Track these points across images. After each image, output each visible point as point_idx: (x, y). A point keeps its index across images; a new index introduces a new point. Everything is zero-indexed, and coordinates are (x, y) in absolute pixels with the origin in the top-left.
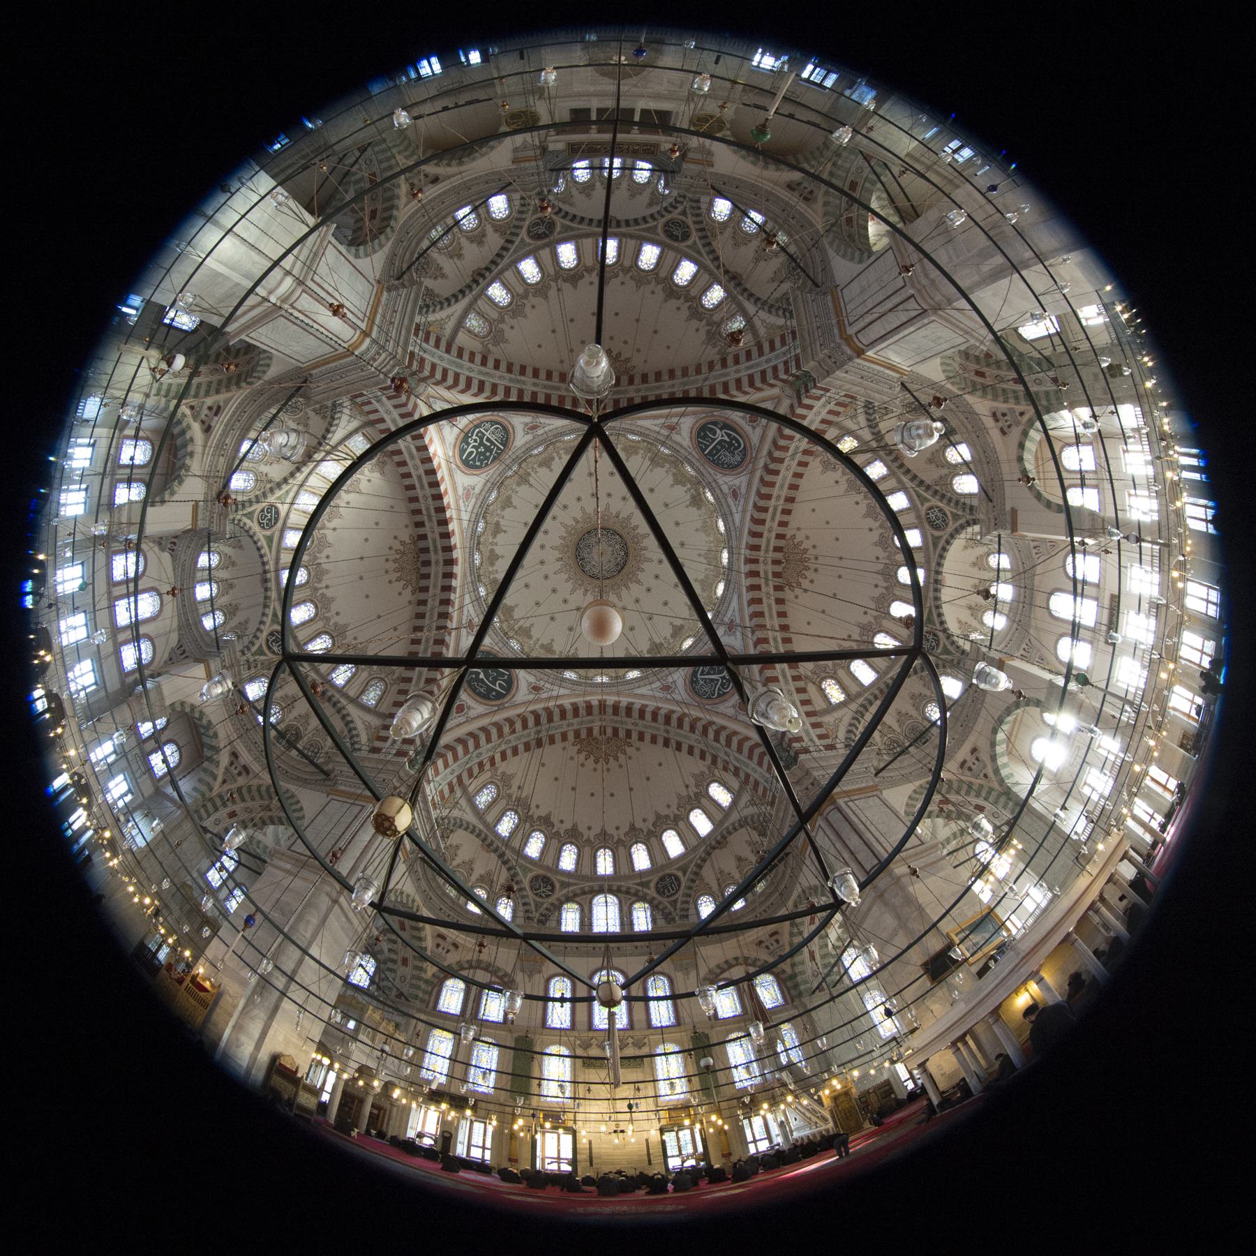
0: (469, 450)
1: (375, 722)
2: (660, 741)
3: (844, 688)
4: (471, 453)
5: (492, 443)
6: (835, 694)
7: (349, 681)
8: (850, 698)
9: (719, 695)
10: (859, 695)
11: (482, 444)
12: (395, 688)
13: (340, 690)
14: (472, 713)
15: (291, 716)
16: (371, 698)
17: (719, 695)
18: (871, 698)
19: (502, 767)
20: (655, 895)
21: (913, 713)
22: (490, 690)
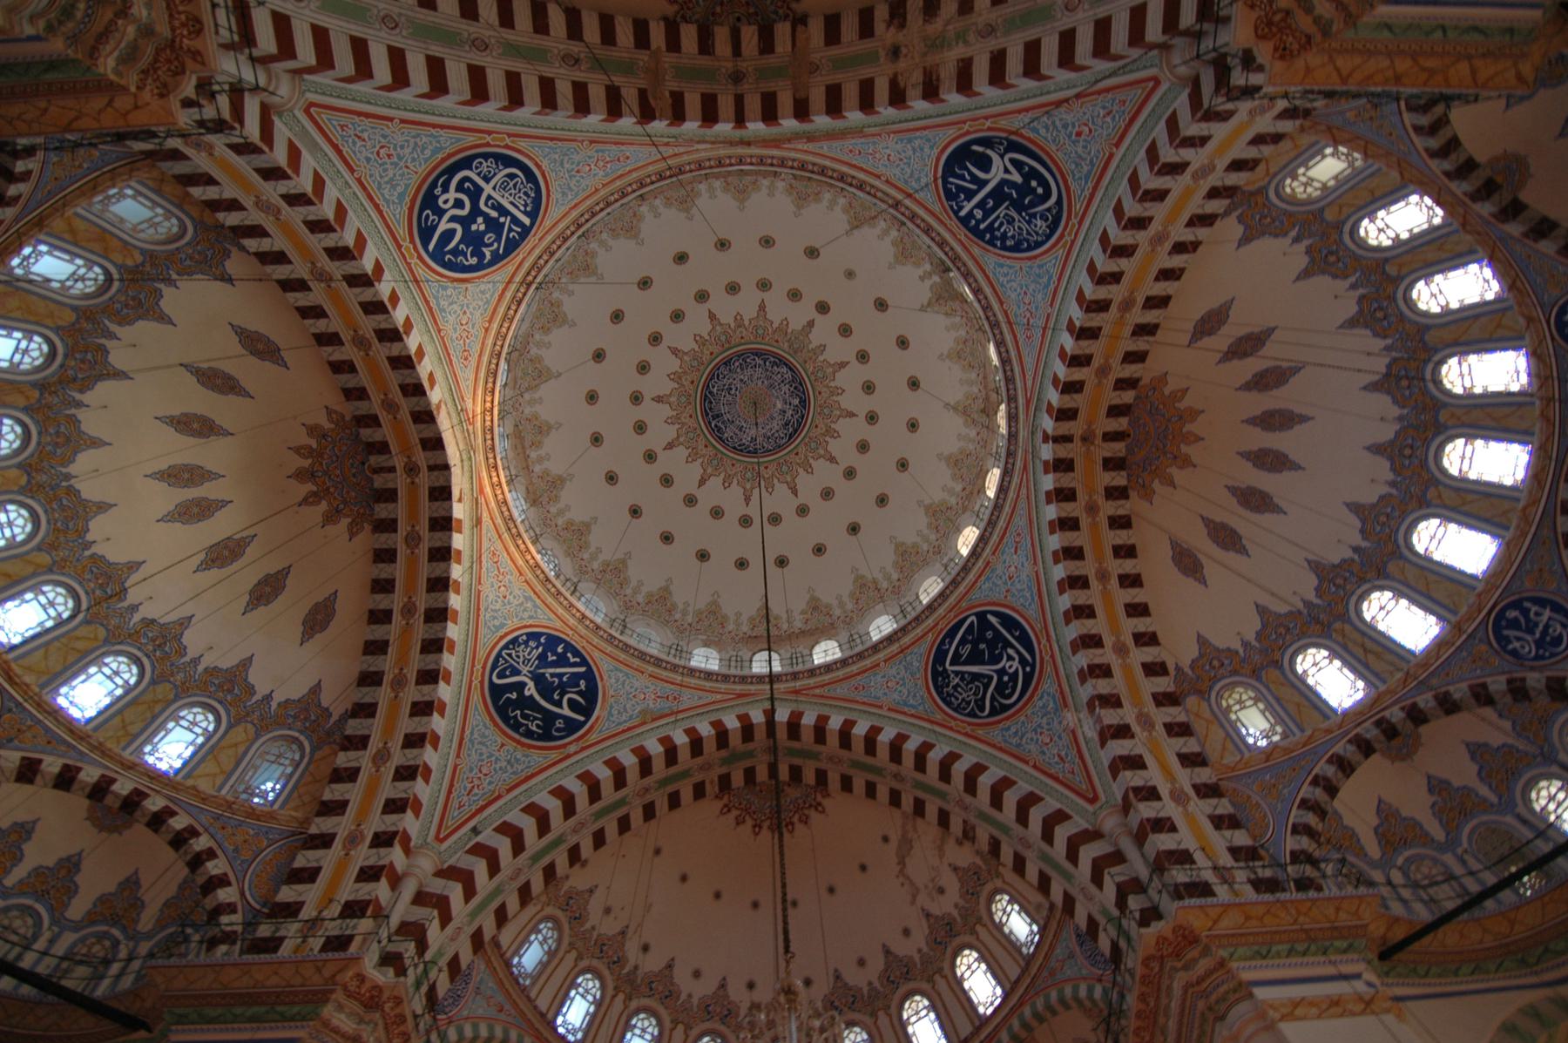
0: (444, 226)
2: (883, 792)
4: (449, 235)
5: (503, 211)
6: (1255, 726)
11: (476, 212)
19: (578, 880)
22: (549, 718)
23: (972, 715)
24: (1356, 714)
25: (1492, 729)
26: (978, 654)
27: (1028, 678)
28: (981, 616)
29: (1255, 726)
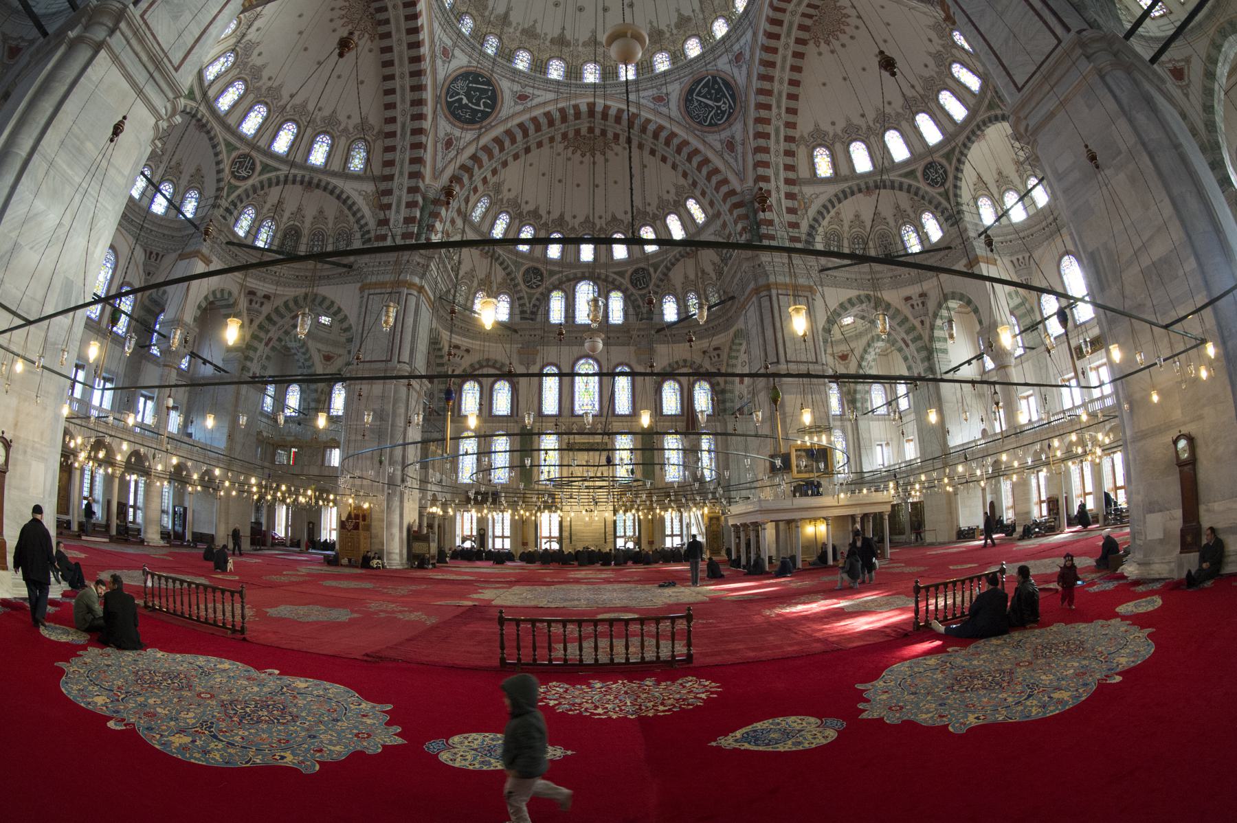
1: (369, 187)
3: (834, 164)
6: (824, 167)
7: (329, 155)
8: (836, 178)
9: (710, 125)
10: (846, 179)
12: (378, 146)
13: (324, 170)
14: (462, 143)
15: (285, 219)
16: (357, 163)
17: (710, 125)
18: (855, 189)
20: (630, 286)
21: (892, 223)
22: (475, 112)
23: (700, 123)
24: (864, 176)
25: (903, 199)
26: (709, 95)
27: (730, 114)
28: (714, 78)
29: (824, 167)
